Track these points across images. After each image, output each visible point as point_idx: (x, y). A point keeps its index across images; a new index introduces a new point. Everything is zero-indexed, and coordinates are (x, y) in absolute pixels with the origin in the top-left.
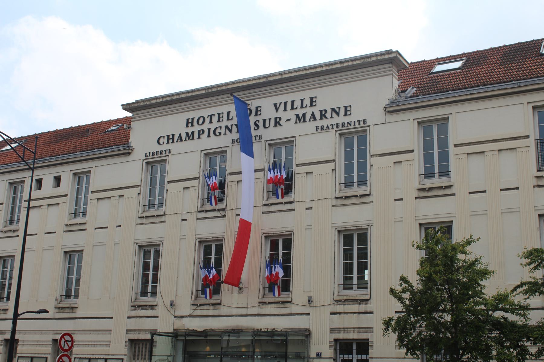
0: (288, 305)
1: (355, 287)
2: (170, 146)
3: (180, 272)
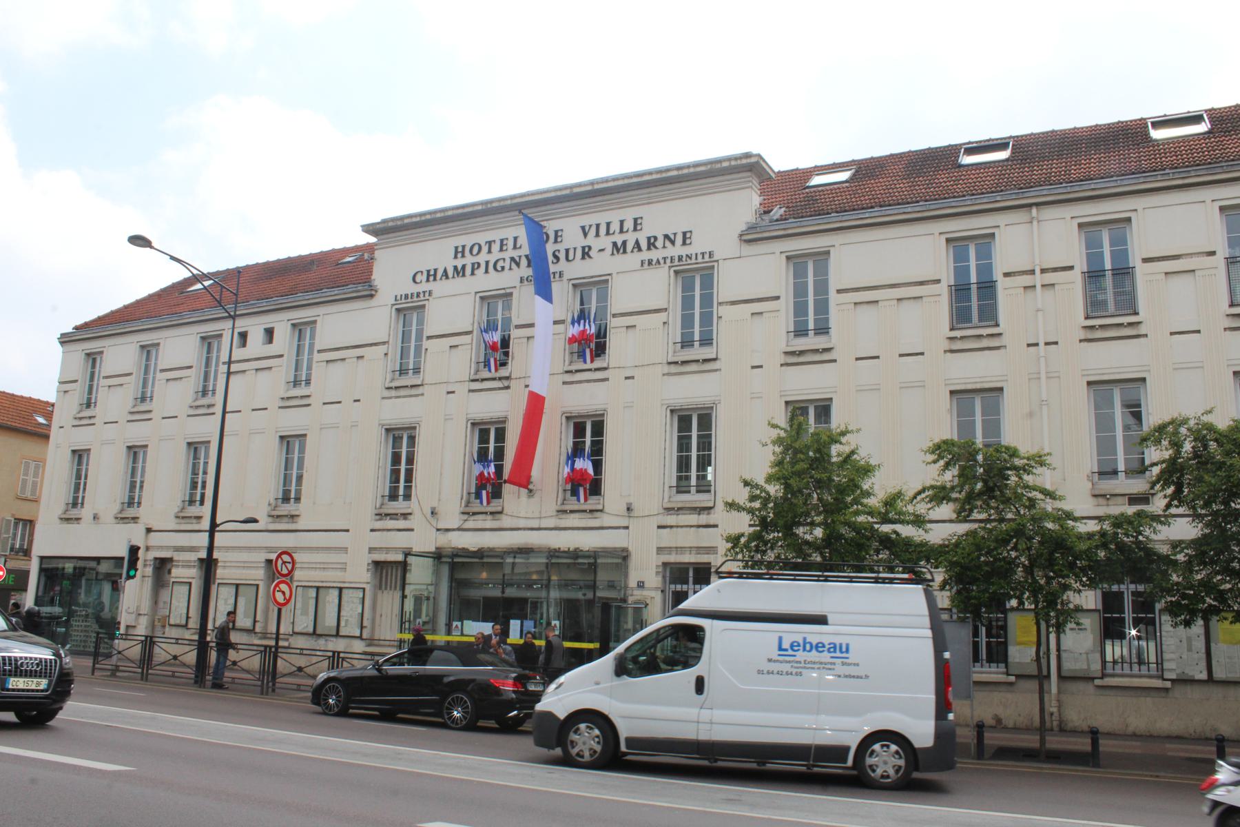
0: (598, 514)
1: (693, 490)
2: (431, 286)
3: (445, 468)
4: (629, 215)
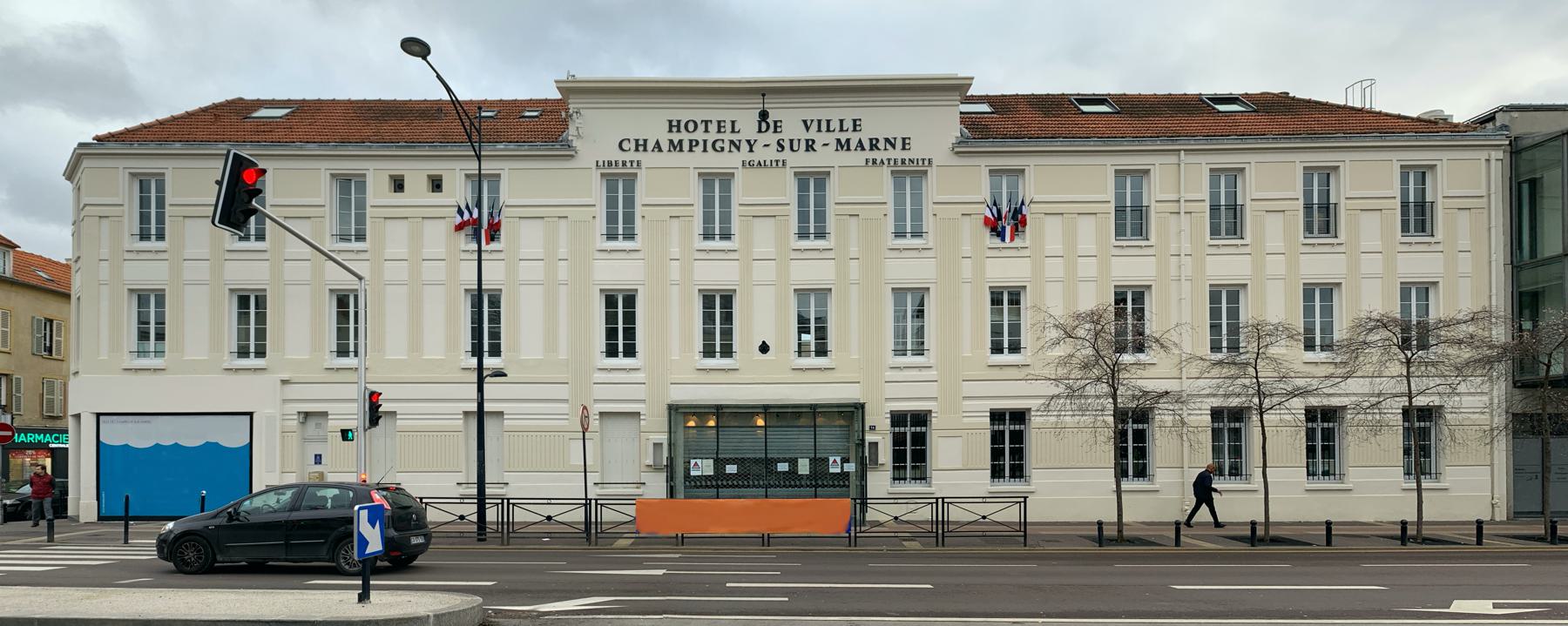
4: (849, 116)
